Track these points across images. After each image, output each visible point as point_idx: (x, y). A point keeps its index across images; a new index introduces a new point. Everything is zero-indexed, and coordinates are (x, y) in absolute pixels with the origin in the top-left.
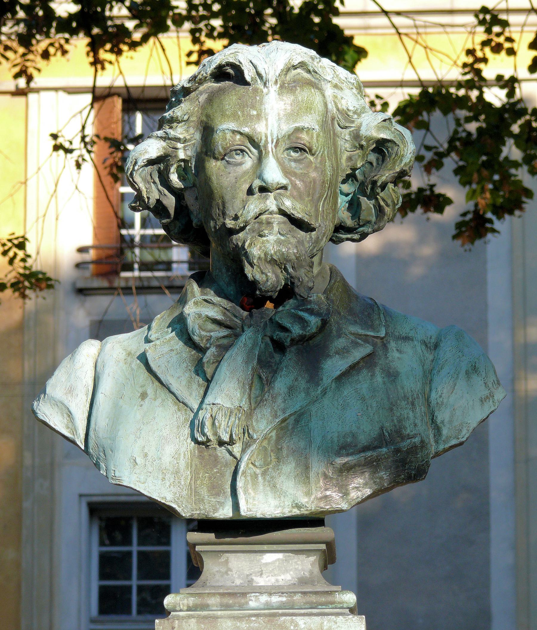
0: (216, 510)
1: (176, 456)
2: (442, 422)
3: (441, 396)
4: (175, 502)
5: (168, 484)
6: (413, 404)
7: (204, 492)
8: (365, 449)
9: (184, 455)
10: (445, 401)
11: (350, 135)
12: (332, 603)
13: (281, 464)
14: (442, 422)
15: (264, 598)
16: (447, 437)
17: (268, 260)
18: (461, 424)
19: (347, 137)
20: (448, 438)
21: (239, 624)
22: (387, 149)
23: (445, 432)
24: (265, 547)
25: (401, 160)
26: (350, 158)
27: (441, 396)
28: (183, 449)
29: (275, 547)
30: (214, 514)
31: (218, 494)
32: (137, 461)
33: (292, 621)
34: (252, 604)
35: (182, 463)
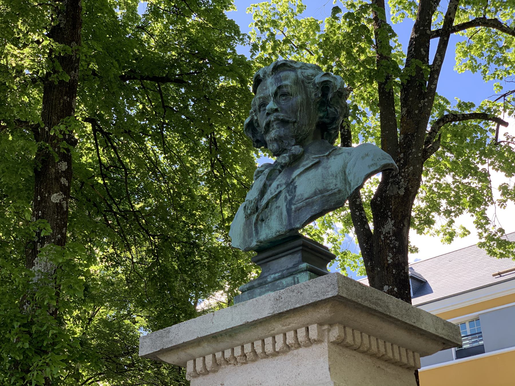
0: (251, 244)
6: (336, 177)
7: (247, 238)
8: (306, 199)
12: (298, 270)
15: (273, 276)
19: (312, 87)
23: (352, 184)
24: (280, 255)
25: (336, 88)
26: (316, 95)
29: (284, 254)
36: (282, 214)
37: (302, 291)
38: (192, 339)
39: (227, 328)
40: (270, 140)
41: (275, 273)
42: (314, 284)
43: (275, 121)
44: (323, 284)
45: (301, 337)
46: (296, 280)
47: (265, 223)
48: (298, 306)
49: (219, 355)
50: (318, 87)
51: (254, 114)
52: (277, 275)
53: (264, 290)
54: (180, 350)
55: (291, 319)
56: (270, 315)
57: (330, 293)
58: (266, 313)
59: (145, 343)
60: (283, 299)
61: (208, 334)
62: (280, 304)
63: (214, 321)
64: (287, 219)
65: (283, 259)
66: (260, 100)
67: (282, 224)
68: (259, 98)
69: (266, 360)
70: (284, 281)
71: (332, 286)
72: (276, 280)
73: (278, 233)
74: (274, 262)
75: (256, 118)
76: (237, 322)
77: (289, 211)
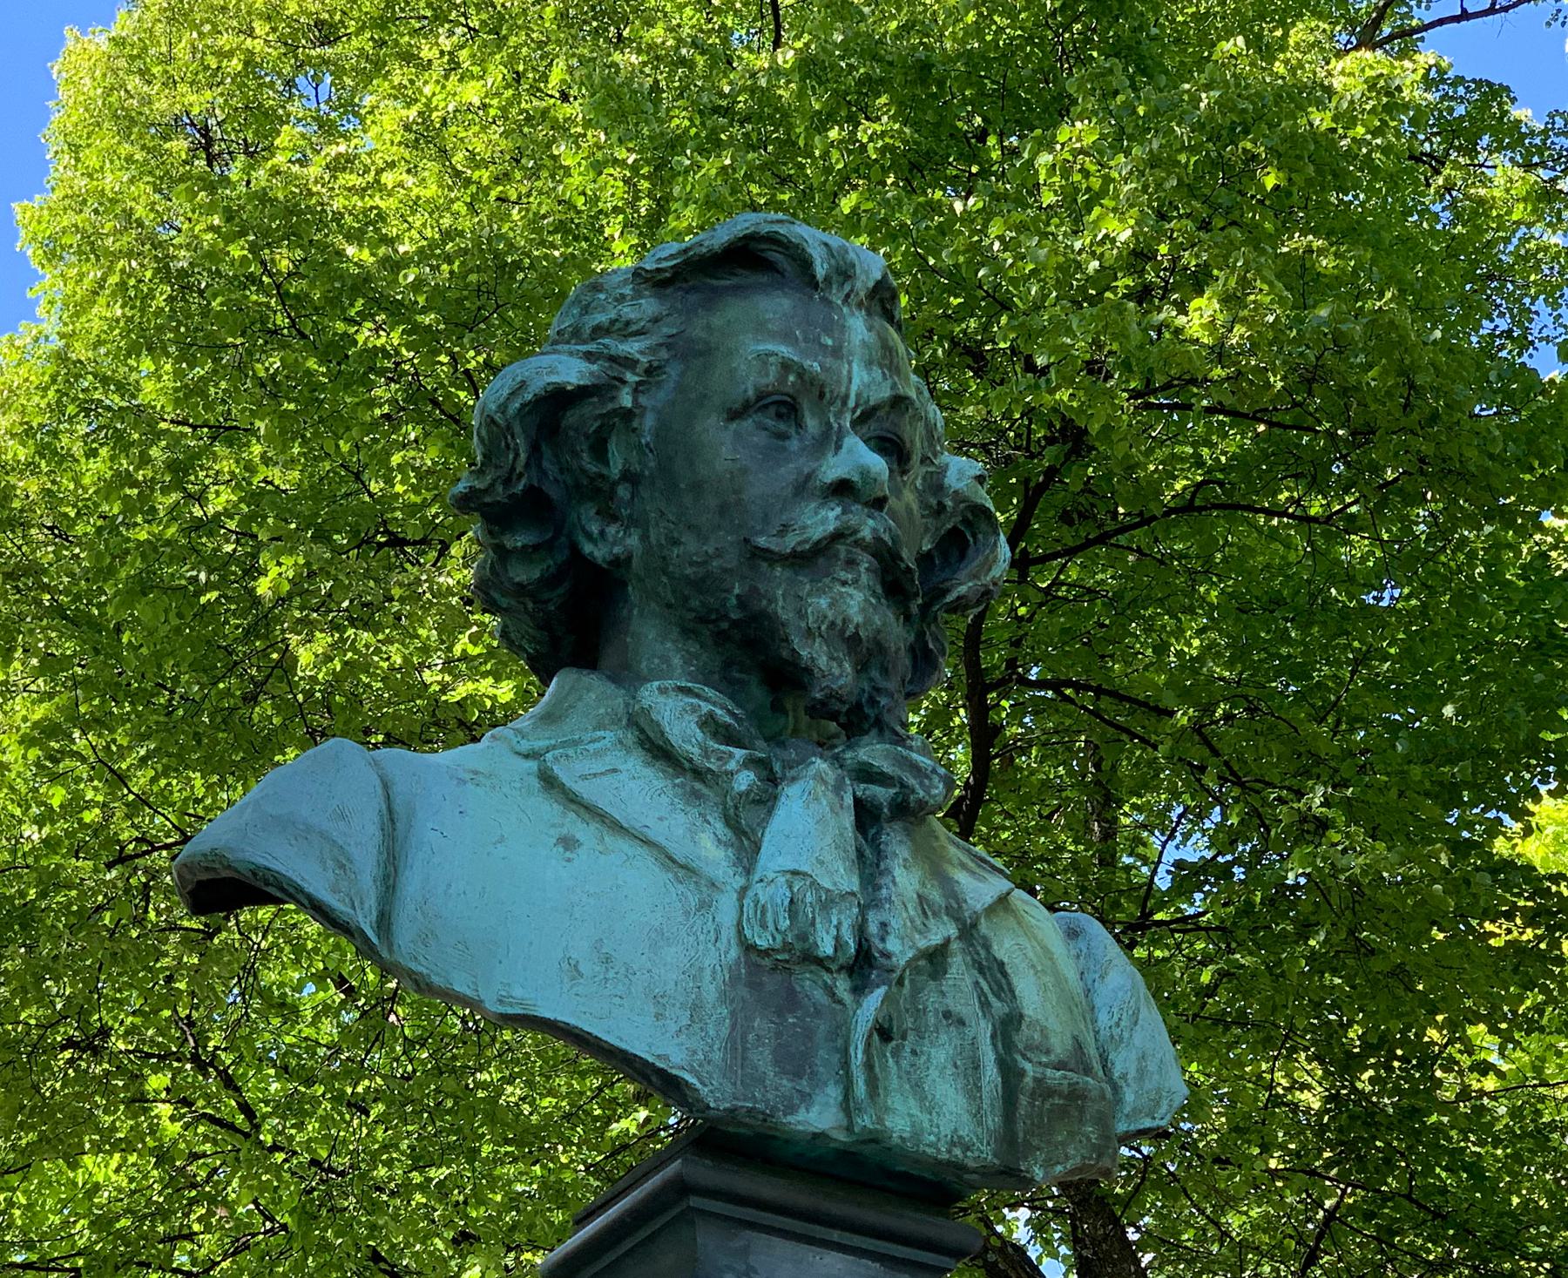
0: (791, 1109)
1: (694, 974)
2: (1124, 1076)
3: (1118, 1025)
4: (692, 1071)
5: (674, 1028)
7: (762, 1059)
9: (714, 972)
10: (1126, 1035)
11: (924, 479)
13: (926, 1041)
14: (1124, 1076)
16: (1134, 1110)
17: (848, 634)
18: (1158, 1091)
20: (1136, 1112)
22: (974, 536)
23: (1129, 1096)
24: (835, 1235)
27: (1118, 1025)
28: (710, 961)
30: (785, 1115)
31: (798, 1075)
32: (581, 968)
35: (710, 992)
36: (976, 1067)
40: (833, 624)
43: (865, 548)
47: (896, 1053)
50: (941, 507)
51: (630, 377)
64: (999, 1104)
66: (782, 379)
67: (977, 1115)
68: (786, 366)
73: (957, 1151)
74: (776, 1241)
75: (626, 400)
77: (1010, 1073)
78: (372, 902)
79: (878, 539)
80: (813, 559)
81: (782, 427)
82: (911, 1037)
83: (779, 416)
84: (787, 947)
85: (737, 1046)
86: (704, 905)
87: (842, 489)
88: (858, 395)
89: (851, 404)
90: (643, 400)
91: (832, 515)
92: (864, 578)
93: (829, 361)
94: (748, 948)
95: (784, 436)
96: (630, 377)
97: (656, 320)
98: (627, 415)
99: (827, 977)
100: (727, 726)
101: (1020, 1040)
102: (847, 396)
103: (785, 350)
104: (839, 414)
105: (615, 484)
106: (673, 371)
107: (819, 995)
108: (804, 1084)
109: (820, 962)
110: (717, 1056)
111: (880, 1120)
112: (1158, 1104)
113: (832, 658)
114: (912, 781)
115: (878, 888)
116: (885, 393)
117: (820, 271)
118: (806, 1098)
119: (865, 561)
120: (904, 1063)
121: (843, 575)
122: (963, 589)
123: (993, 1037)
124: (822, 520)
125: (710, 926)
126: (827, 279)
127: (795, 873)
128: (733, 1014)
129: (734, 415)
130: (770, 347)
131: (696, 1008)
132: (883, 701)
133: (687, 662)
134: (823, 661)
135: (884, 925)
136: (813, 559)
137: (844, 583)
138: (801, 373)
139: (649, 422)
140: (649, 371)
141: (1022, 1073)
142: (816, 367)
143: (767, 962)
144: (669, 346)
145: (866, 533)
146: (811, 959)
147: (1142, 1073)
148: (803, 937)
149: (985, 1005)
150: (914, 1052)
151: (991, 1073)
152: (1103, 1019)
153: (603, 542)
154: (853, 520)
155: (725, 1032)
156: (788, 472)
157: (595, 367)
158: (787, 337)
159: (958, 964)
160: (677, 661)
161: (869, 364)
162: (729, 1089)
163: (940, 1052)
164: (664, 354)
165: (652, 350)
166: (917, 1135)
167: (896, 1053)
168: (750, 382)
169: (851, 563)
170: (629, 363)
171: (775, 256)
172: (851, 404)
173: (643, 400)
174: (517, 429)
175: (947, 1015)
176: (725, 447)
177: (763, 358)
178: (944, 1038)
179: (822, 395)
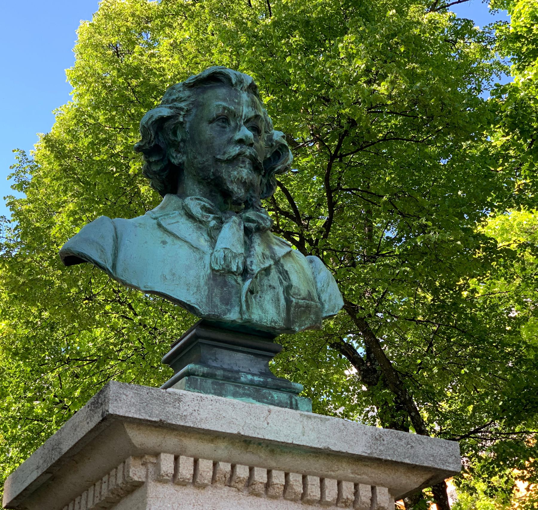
1: (198, 277)
2: (325, 301)
4: (197, 304)
5: (192, 293)
7: (217, 300)
14: (325, 301)
15: (250, 377)
18: (335, 304)
21: (238, 389)
23: (326, 306)
24: (240, 348)
28: (202, 273)
29: (246, 349)
31: (227, 304)
32: (167, 277)
33: (270, 394)
34: (243, 379)
35: (202, 282)
37: (413, 444)
38: (228, 431)
39: (295, 442)
41: (253, 375)
42: (430, 444)
43: (248, 157)
44: (442, 450)
45: (364, 496)
46: (294, 402)
47: (255, 298)
48: (407, 461)
49: (225, 467)
50: (272, 145)
51: (182, 113)
52: (256, 379)
53: (241, 391)
54: (176, 433)
55: (370, 469)
56: (366, 455)
57: (451, 466)
58: (359, 450)
59: (124, 396)
60: (385, 442)
61: (260, 436)
62: (382, 448)
63: (270, 421)
64: (285, 310)
65: (240, 356)
66: (223, 112)
67: (279, 314)
68: (224, 108)
69: (293, 503)
70: (276, 395)
71: (454, 458)
72: (252, 383)
73: (273, 324)
74: (223, 351)
75: (181, 119)
76: (310, 440)
77: (288, 302)
78: (111, 261)
79: (251, 155)
80: (233, 161)
81: (224, 125)
82: (259, 292)
83: (223, 122)
84: (223, 269)
85: (210, 297)
86: (201, 258)
87: (241, 142)
88: (245, 115)
89: (243, 117)
90: (186, 119)
91: (237, 149)
92: (247, 166)
93: (236, 106)
94: (213, 270)
95: (224, 127)
96: (182, 113)
97: (189, 97)
98: (182, 123)
99: (235, 277)
100: (209, 208)
101: (291, 292)
102: (242, 116)
103: (224, 104)
104: (240, 121)
105: (179, 142)
106: (194, 111)
107: (233, 282)
108: (229, 307)
109: (233, 273)
110: (204, 300)
111: (250, 316)
112: (335, 308)
113: (238, 188)
114: (261, 221)
115: (250, 252)
116: (252, 114)
117: (234, 81)
118: (229, 311)
119: (247, 161)
120: (257, 300)
121: (241, 165)
122: (279, 167)
123: (283, 292)
124: (235, 150)
125: (203, 264)
126: (236, 84)
127: (226, 248)
128: (209, 288)
129: (211, 122)
130: (220, 103)
131: (198, 287)
132: (254, 199)
133: (200, 191)
134: (236, 189)
135: (251, 262)
136: (233, 161)
137: (241, 167)
138: (229, 110)
139: (188, 125)
140: (187, 111)
141: (292, 301)
142: (233, 108)
143: (218, 273)
144: (192, 104)
145: (247, 153)
146: (230, 272)
147: (330, 299)
148: (228, 266)
149: (281, 283)
150: (260, 297)
151: (283, 302)
152: (319, 285)
153: (177, 159)
154: (243, 150)
155: (206, 293)
156: (225, 137)
157: (172, 111)
158: (225, 100)
159: (274, 273)
160: (197, 191)
161: (248, 106)
162: (208, 309)
163: (268, 297)
164: (191, 106)
165: (188, 105)
166: (261, 320)
167: (255, 298)
168: (214, 112)
169: (243, 162)
170: (181, 109)
171: (221, 78)
172: (243, 117)
173: (186, 119)
174: (151, 128)
175: (270, 286)
176: (208, 131)
177: (218, 106)
178: (269, 292)
179: (235, 116)
